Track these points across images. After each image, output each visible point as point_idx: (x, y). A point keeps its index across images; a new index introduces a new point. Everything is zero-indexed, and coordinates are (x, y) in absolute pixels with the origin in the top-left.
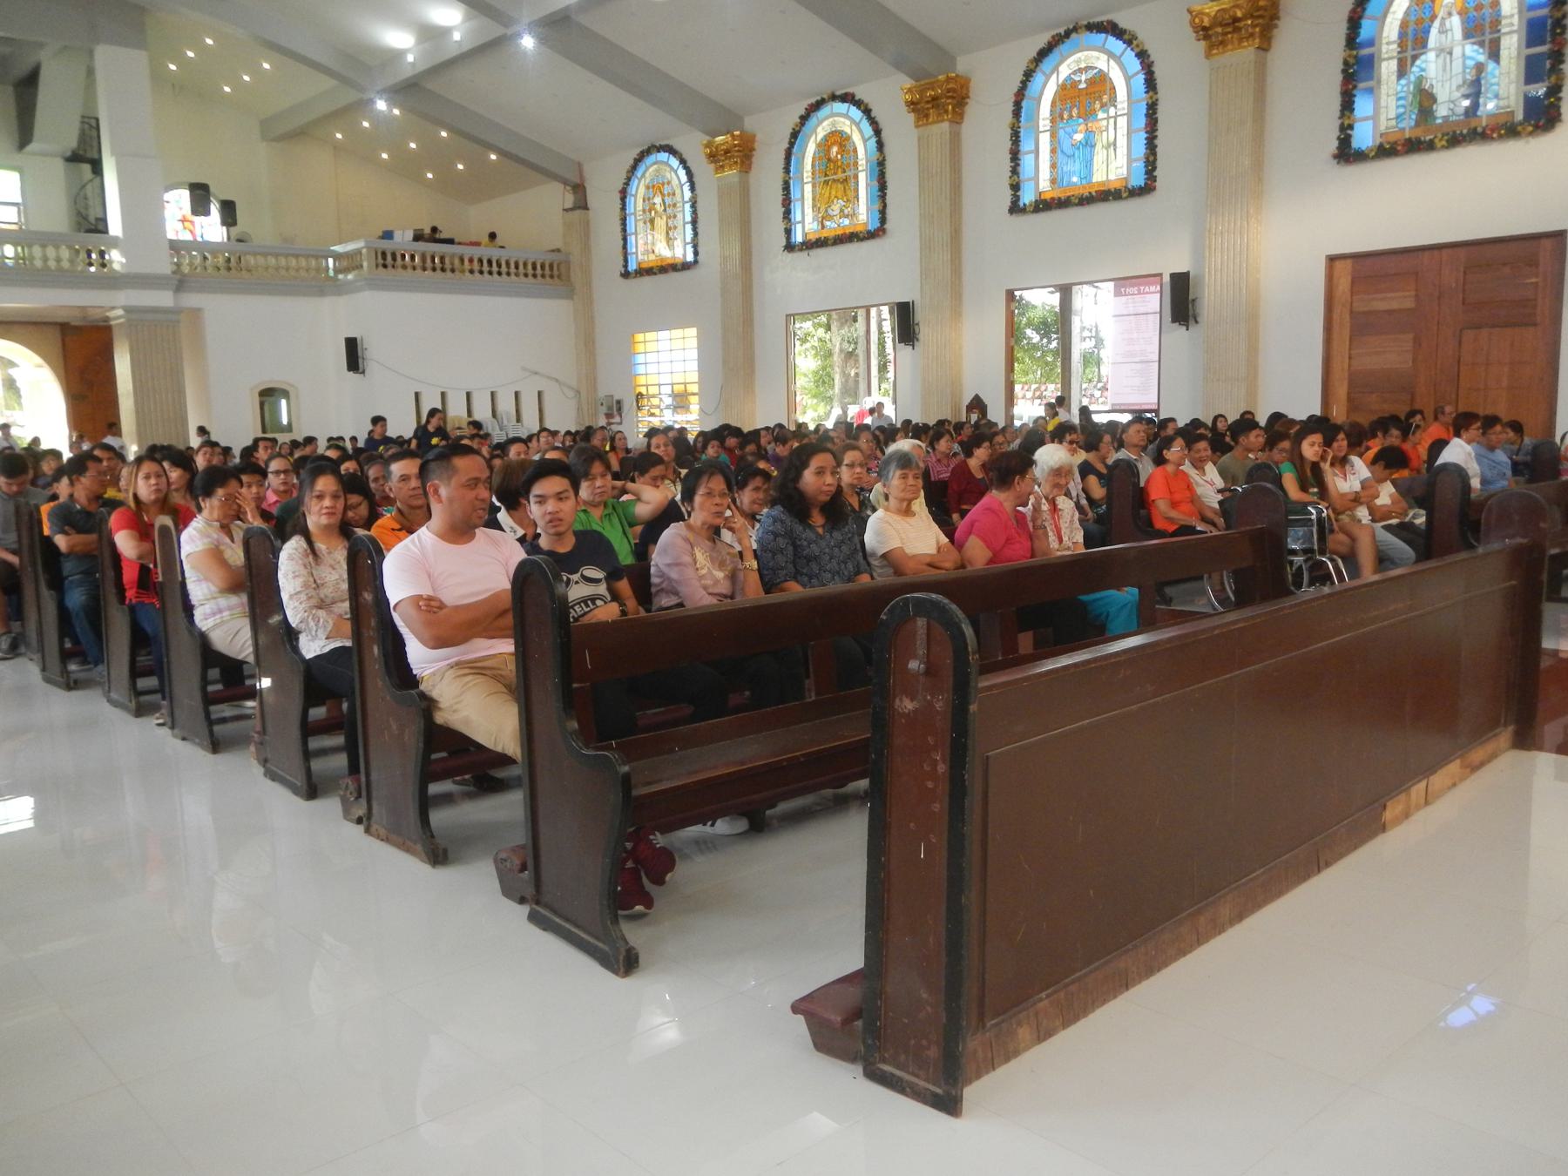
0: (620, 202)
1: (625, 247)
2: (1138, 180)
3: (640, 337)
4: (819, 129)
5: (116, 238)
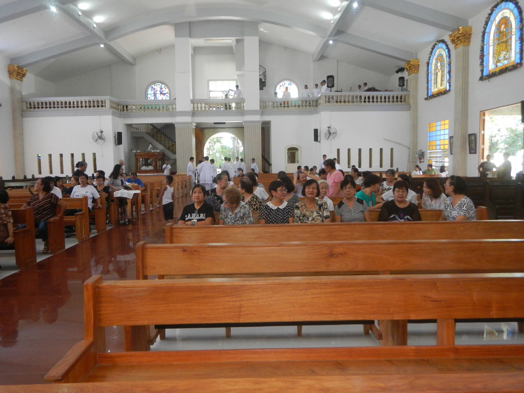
0: (427, 67)
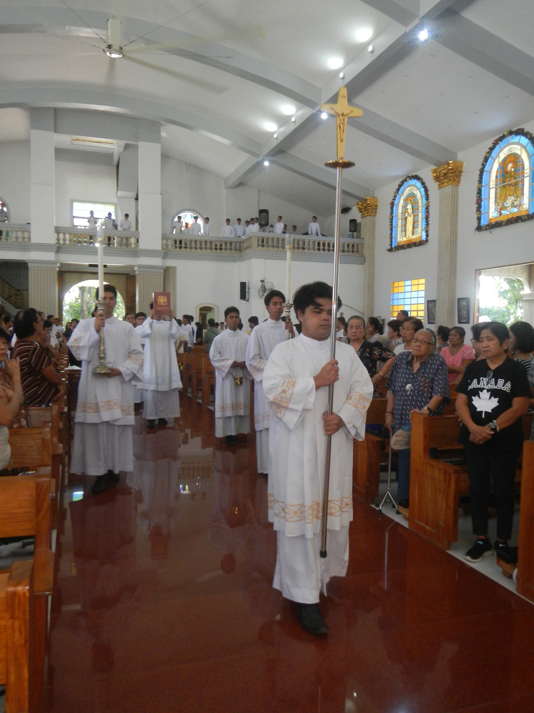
0: (390, 209)
1: (391, 234)
3: (396, 284)
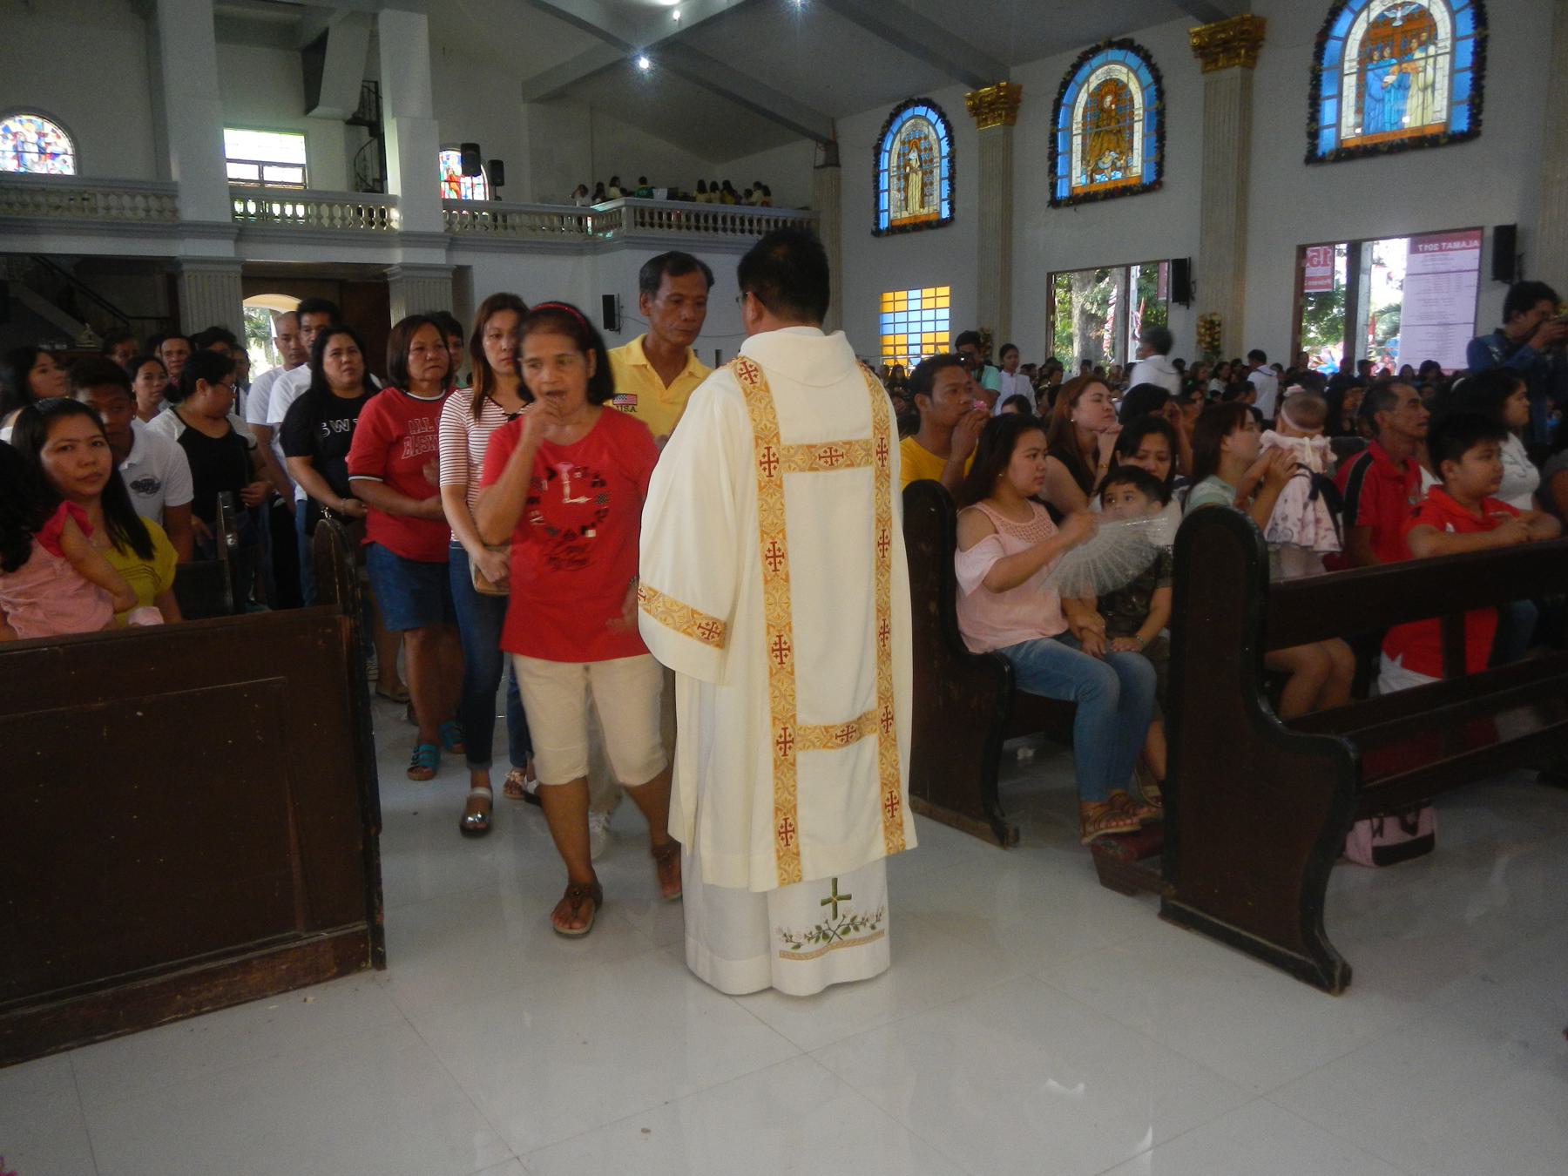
0: (873, 158)
2: (1462, 124)
3: (888, 296)
4: (1093, 78)
5: (394, 197)
